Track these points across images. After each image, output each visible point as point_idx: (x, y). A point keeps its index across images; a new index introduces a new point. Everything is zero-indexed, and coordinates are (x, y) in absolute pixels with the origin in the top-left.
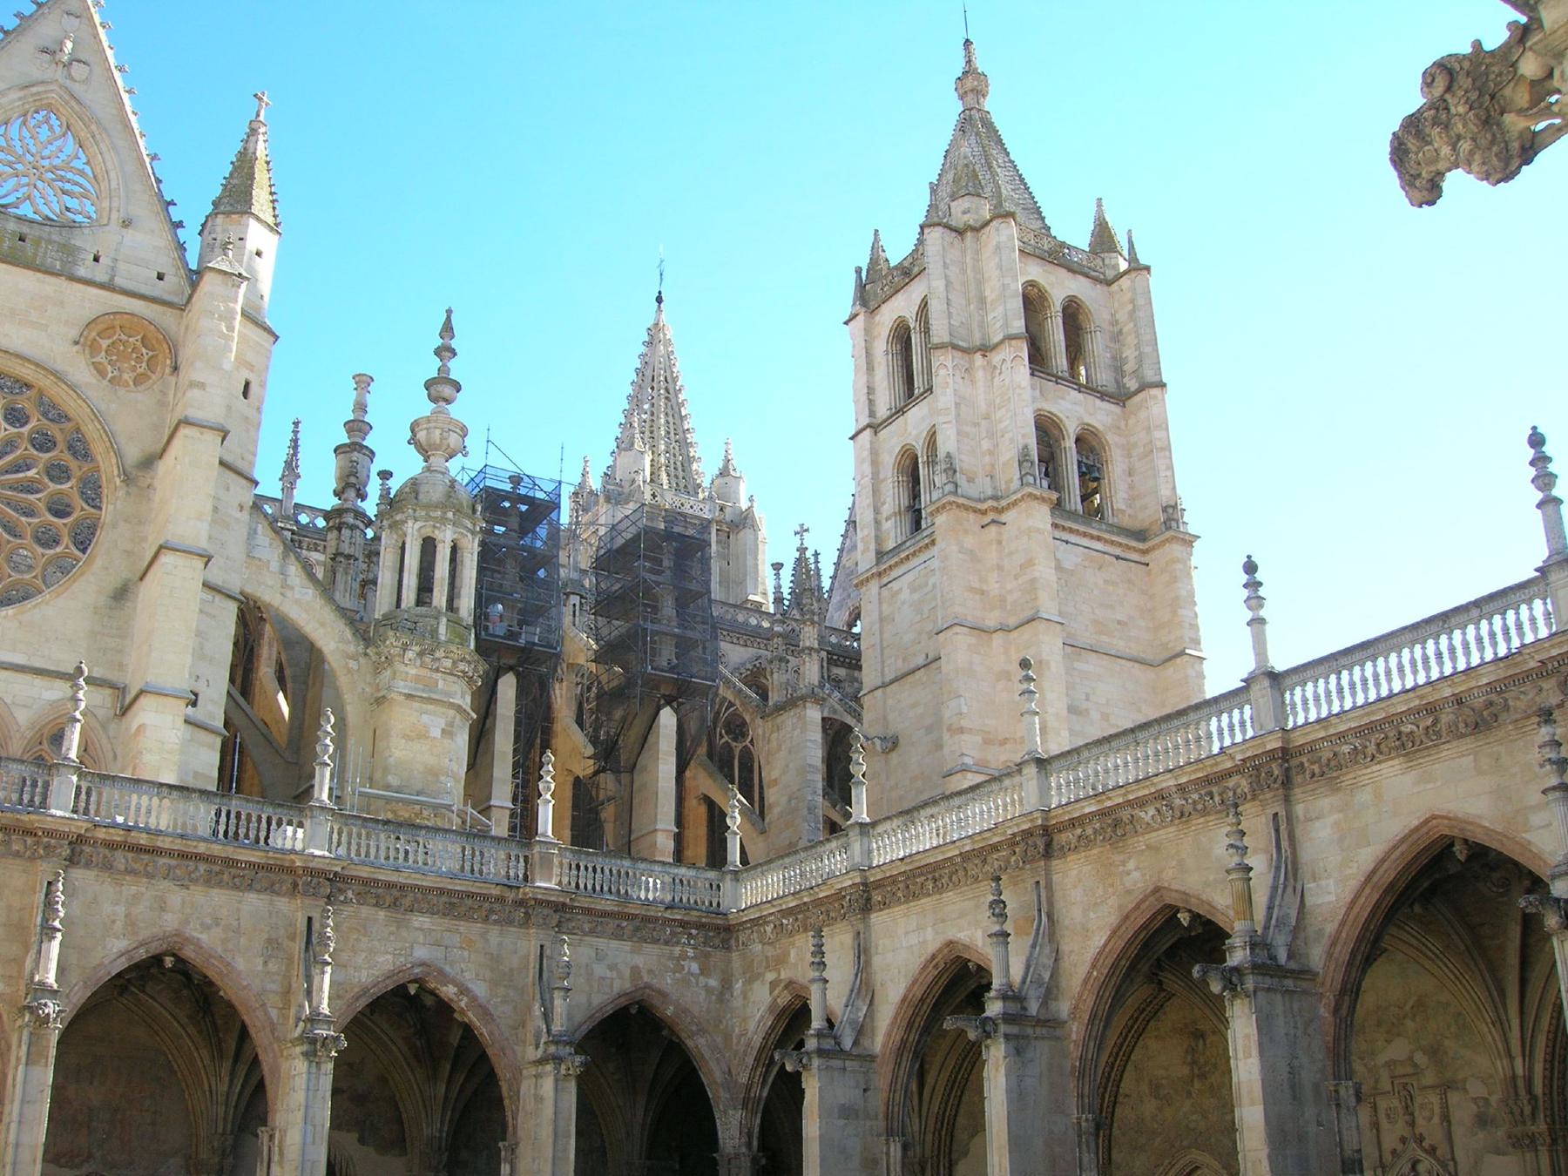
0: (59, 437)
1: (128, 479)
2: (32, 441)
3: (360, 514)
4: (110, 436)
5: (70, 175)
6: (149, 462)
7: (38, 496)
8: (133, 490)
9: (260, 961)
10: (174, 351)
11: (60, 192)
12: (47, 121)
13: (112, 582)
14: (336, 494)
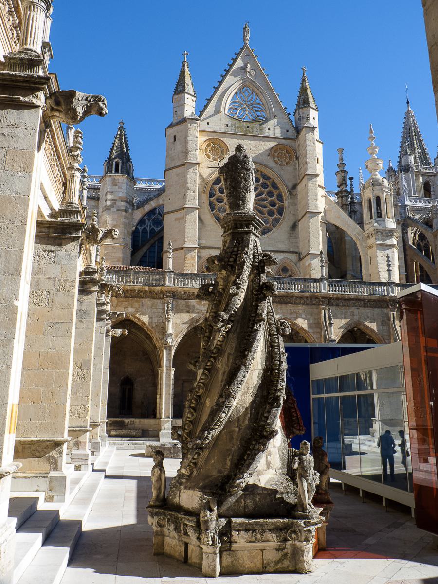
0: (269, 184)
1: (291, 193)
2: (262, 186)
3: (346, 191)
4: (283, 181)
5: (256, 105)
6: (295, 187)
7: (267, 202)
8: (292, 196)
9: (381, 327)
10: (295, 152)
11: (255, 111)
12: (247, 90)
13: (291, 223)
14: (339, 187)
